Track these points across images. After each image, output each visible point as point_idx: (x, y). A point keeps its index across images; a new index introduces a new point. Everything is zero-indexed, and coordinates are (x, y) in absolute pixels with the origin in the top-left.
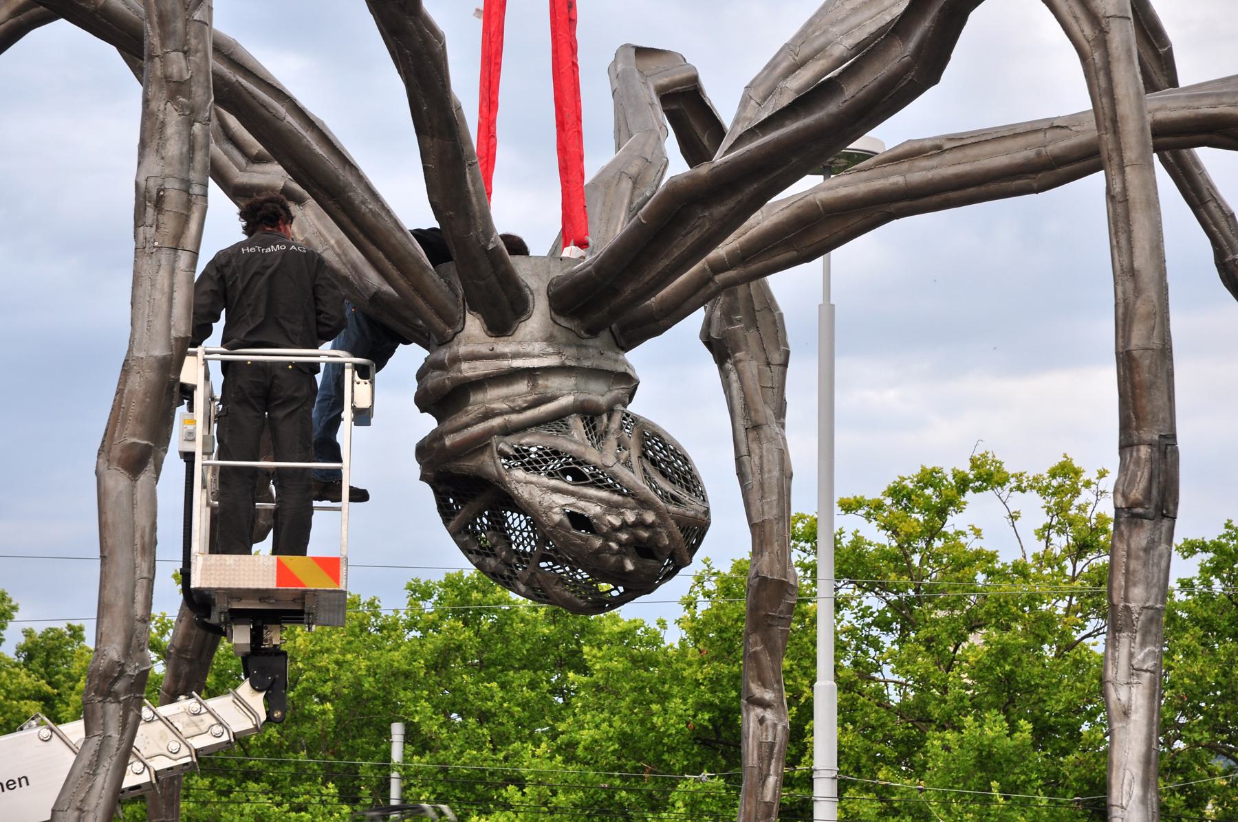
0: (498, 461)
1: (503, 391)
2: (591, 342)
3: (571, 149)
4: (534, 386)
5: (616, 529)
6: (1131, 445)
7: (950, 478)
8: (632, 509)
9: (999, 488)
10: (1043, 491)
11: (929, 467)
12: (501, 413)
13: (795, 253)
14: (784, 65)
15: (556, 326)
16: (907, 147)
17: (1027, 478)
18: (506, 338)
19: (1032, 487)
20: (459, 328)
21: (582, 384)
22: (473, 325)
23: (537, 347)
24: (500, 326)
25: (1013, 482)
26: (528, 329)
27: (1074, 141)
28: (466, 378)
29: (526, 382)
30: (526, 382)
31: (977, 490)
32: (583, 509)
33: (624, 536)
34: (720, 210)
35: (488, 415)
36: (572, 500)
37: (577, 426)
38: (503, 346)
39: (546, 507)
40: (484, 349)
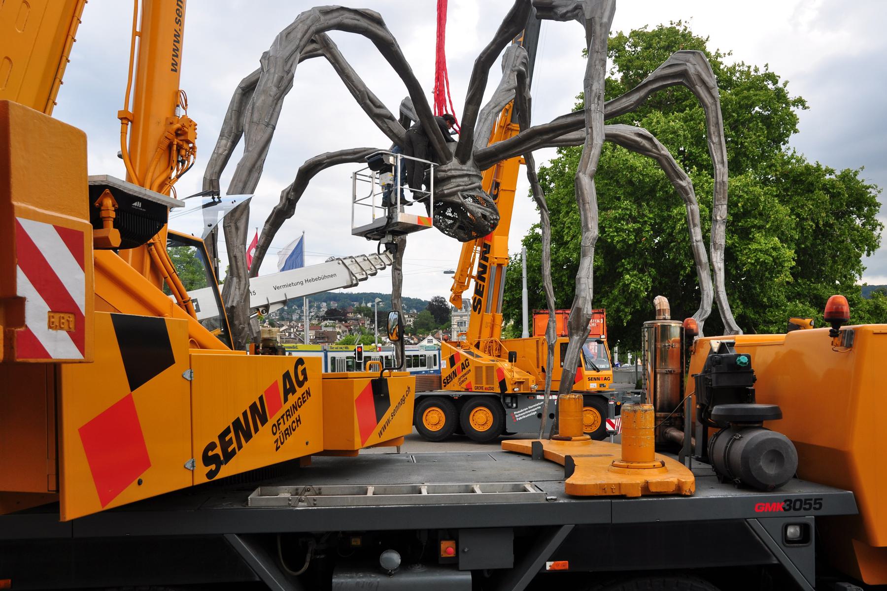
5: (491, 219)
14: (493, 106)
22: (454, 162)
24: (463, 162)
33: (492, 222)
38: (464, 167)
40: (459, 168)
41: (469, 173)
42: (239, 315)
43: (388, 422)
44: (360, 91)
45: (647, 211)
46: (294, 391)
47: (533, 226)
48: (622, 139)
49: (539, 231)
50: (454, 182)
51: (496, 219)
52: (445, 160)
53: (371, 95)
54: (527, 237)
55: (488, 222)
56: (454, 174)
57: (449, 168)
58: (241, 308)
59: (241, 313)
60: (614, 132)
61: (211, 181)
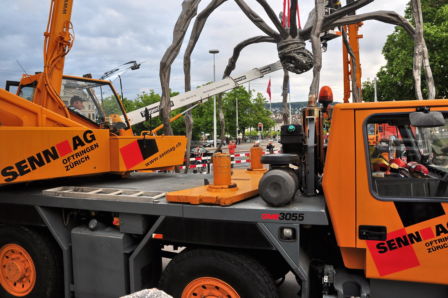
1: (293, 45)
3: (264, 26)
5: (309, 63)
6: (419, 45)
12: (294, 48)
22: (290, 37)
23: (298, 40)
24: (294, 37)
27: (361, 18)
34: (331, 21)
40: (292, 40)
41: (296, 42)
42: (165, 112)
43: (156, 159)
44: (247, 11)
45: (437, 56)
46: (83, 144)
47: (381, 67)
48: (380, 18)
49: (385, 69)
50: (290, 47)
51: (311, 62)
52: (285, 37)
53: (253, 13)
54: (378, 73)
55: (307, 64)
56: (290, 43)
57: (287, 40)
58: (165, 109)
59: (166, 111)
60: (376, 15)
61: (187, 57)
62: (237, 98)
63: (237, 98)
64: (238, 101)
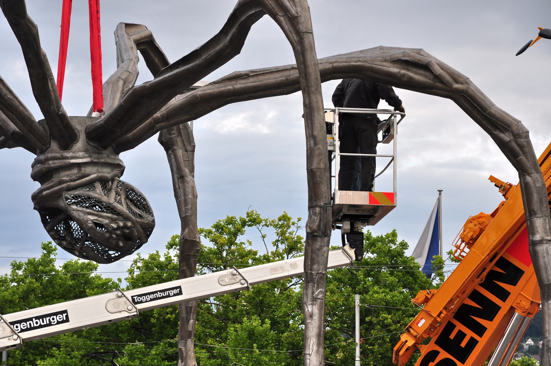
0: (65, 202)
1: (68, 173)
2: (104, 152)
4: (80, 170)
7: (239, 221)
8: (121, 221)
9: (258, 225)
10: (276, 226)
11: (230, 216)
13: (189, 116)
15: (89, 145)
16: (234, 74)
17: (269, 221)
18: (68, 151)
19: (271, 225)
20: (48, 146)
21: (100, 169)
22: (54, 145)
24: (66, 145)
25: (264, 223)
26: (77, 147)
28: (51, 167)
29: (77, 169)
30: (77, 169)
31: (249, 226)
32: (101, 221)
35: (61, 182)
36: (96, 218)
37: (98, 186)
39: (85, 221)
62: (357, 298)
63: (357, 298)
64: (364, 313)
